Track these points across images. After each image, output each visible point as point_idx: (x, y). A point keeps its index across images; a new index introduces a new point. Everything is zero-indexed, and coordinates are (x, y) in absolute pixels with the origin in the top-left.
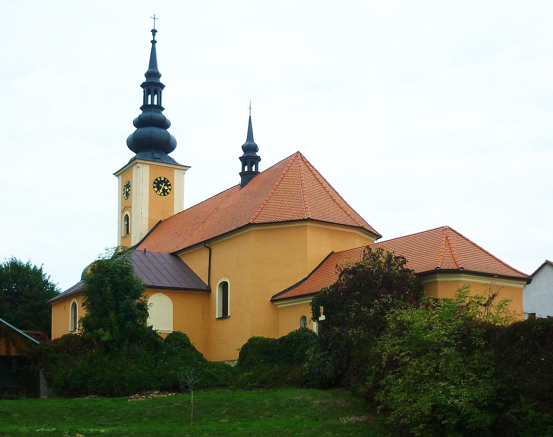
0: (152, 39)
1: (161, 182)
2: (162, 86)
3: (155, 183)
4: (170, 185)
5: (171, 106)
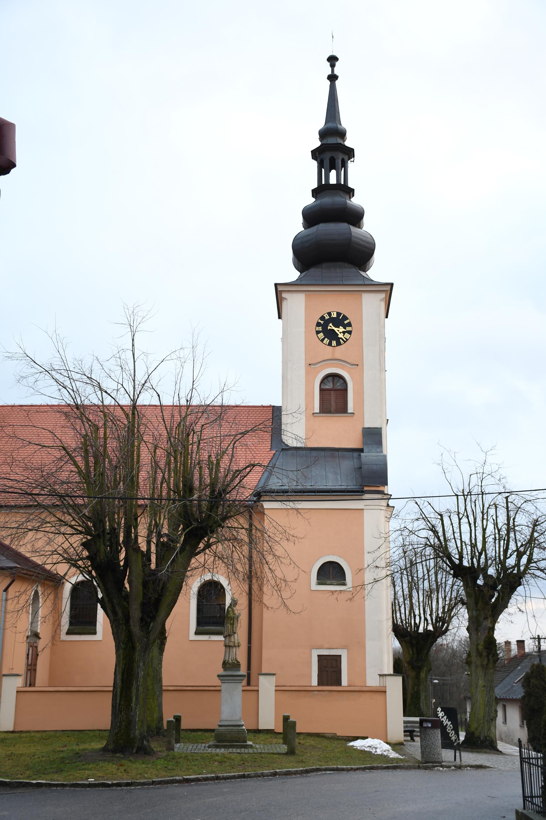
0: (330, 73)
1: (327, 322)
2: (350, 153)
3: (318, 324)
4: (349, 324)
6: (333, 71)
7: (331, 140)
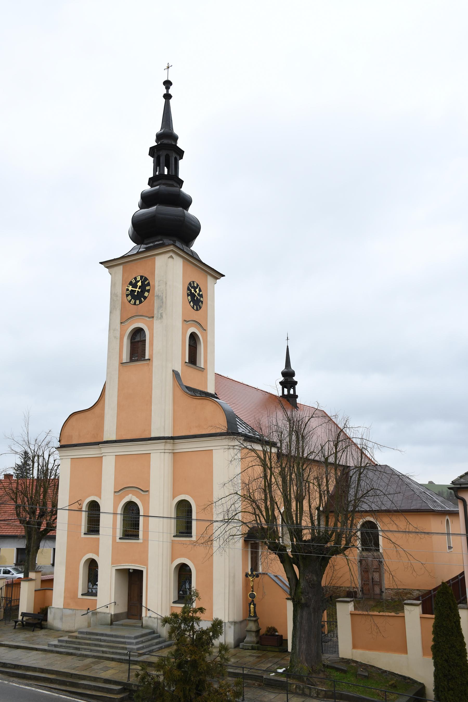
5: (191, 175)
6: (167, 91)
7: (166, 141)
